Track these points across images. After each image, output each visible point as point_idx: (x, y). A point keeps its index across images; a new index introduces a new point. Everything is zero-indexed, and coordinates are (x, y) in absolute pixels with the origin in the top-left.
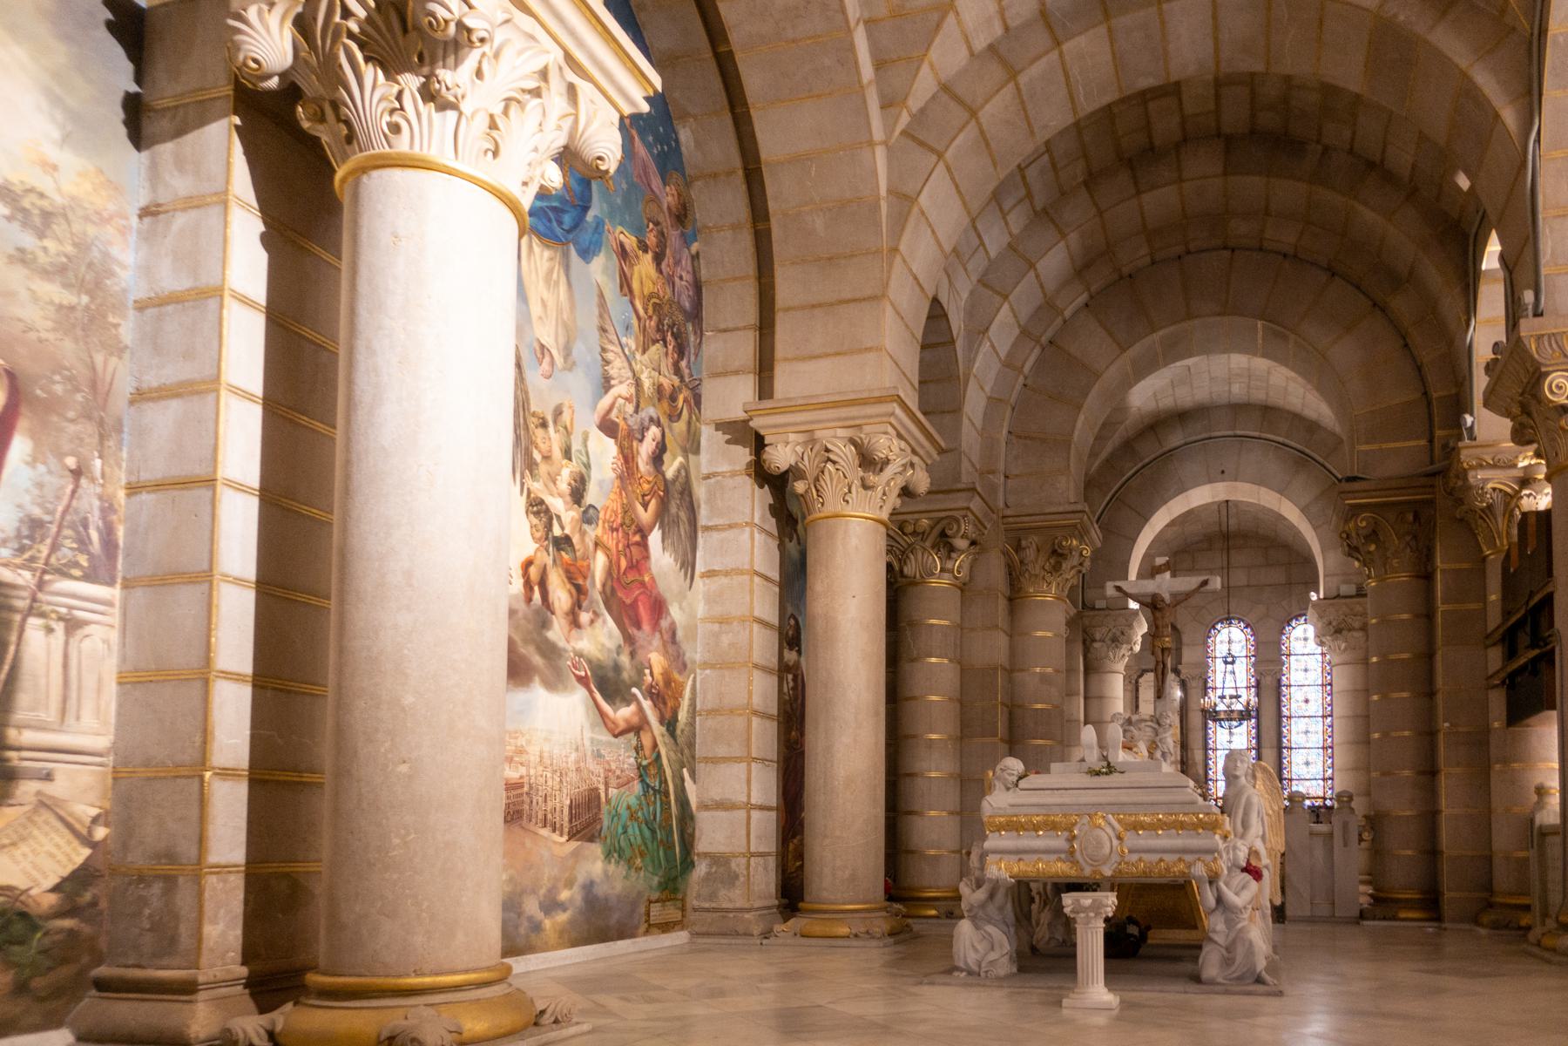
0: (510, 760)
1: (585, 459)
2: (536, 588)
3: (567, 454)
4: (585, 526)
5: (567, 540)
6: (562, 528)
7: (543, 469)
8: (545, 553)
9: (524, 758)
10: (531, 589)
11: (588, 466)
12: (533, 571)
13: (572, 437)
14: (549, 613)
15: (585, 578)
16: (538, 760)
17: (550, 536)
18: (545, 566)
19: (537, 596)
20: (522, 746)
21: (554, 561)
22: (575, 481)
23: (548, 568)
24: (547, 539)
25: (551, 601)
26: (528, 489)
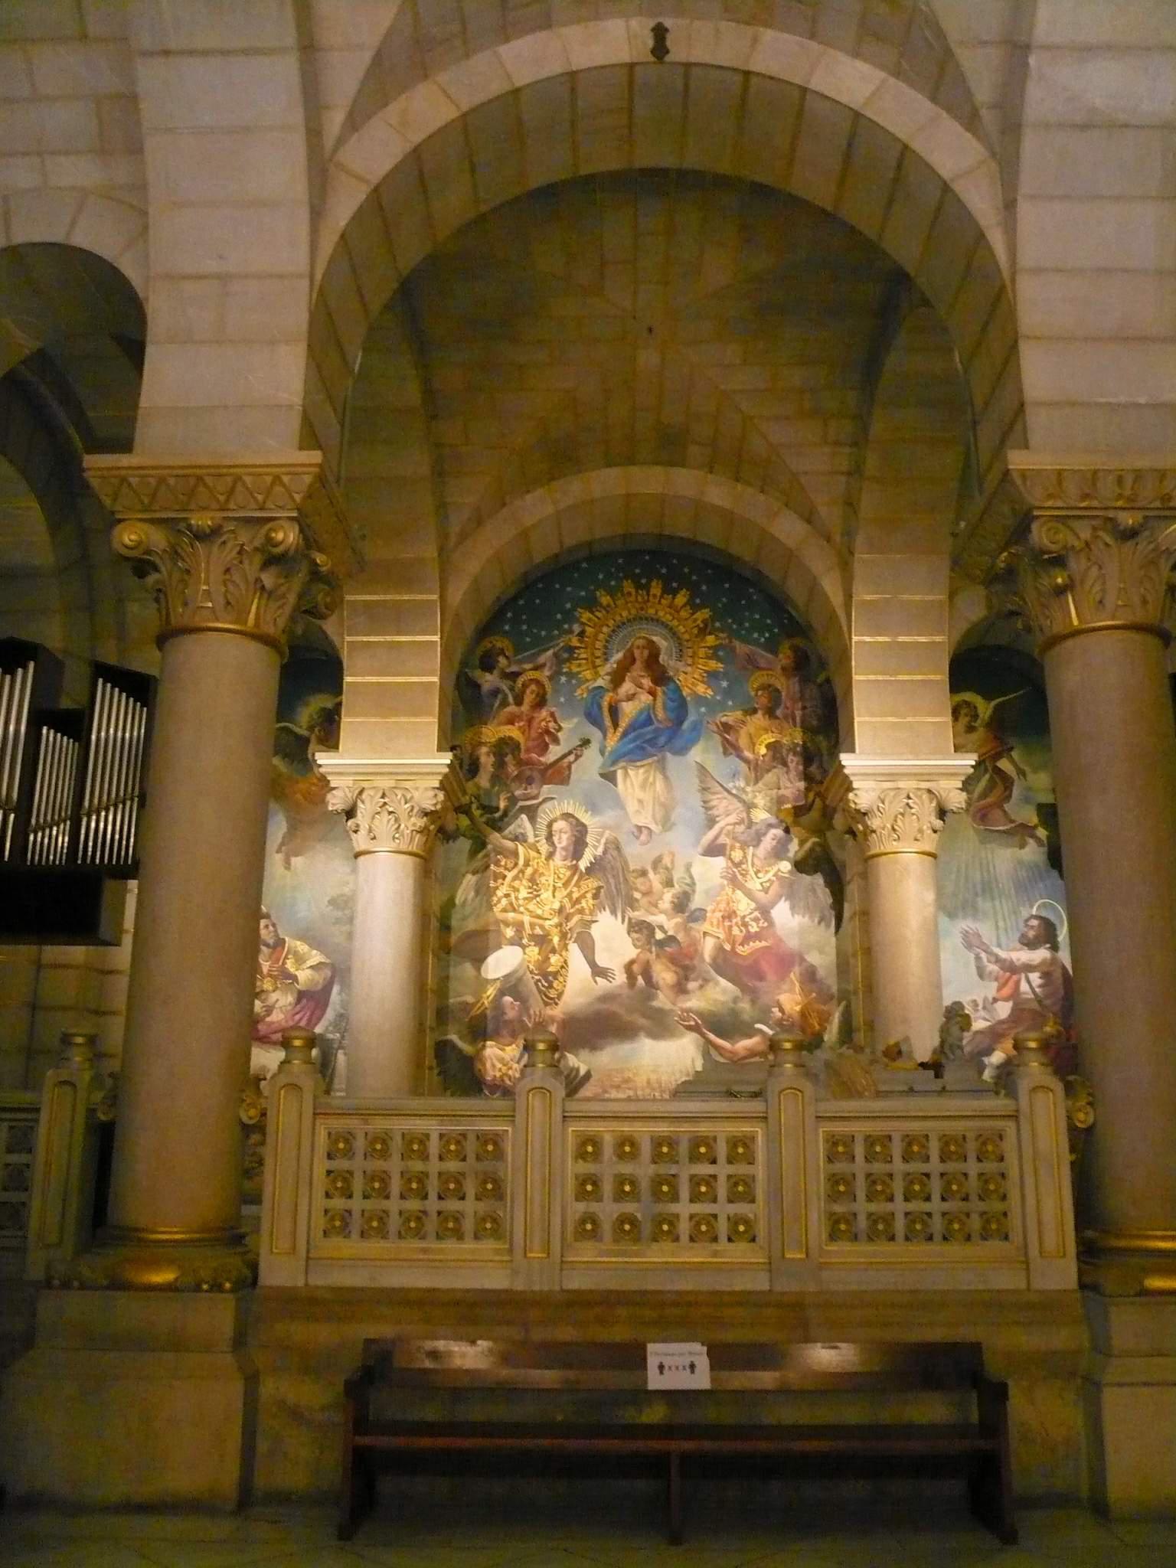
0: (618, 1087)
1: (688, 881)
2: (640, 978)
3: (669, 883)
4: (691, 925)
5: (671, 939)
6: (665, 932)
7: (644, 901)
8: (648, 953)
9: (630, 1085)
10: (636, 979)
11: (693, 884)
12: (636, 968)
13: (673, 872)
14: (654, 991)
15: (692, 959)
16: (645, 1084)
17: (653, 940)
18: (648, 962)
19: (640, 981)
20: (629, 1078)
21: (658, 956)
22: (678, 898)
23: (651, 962)
24: (649, 943)
25: (654, 980)
26: (630, 919)
